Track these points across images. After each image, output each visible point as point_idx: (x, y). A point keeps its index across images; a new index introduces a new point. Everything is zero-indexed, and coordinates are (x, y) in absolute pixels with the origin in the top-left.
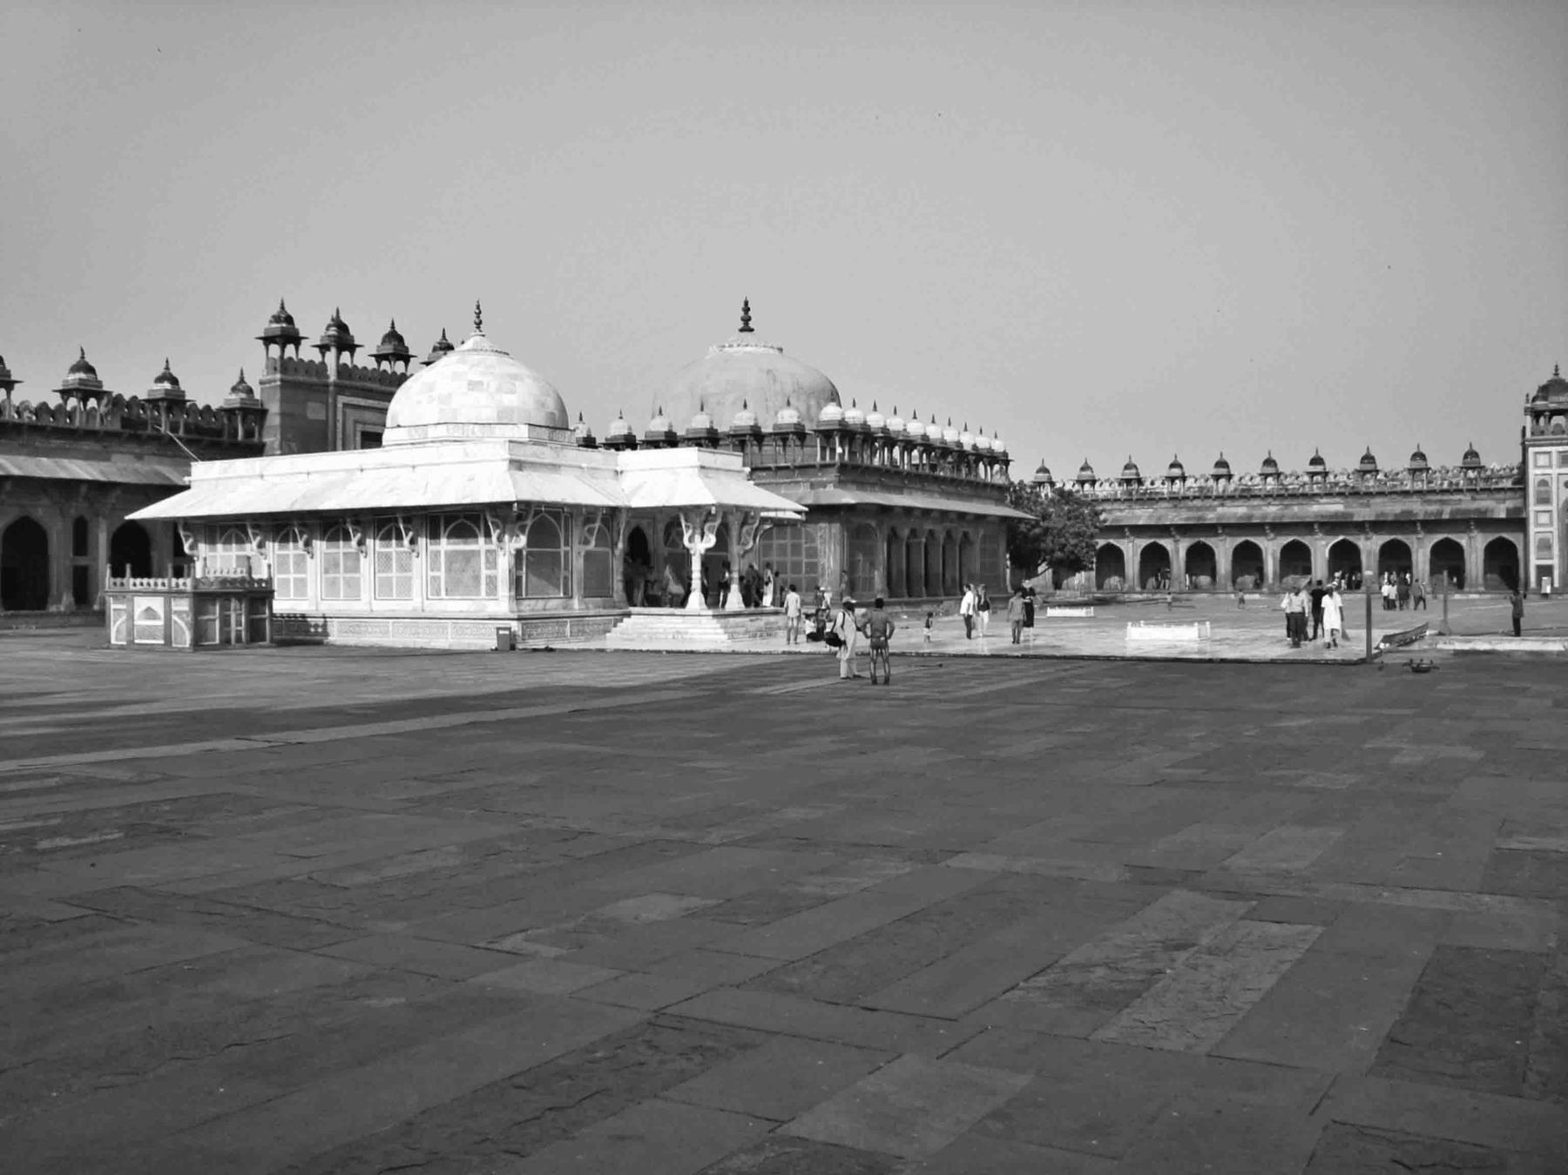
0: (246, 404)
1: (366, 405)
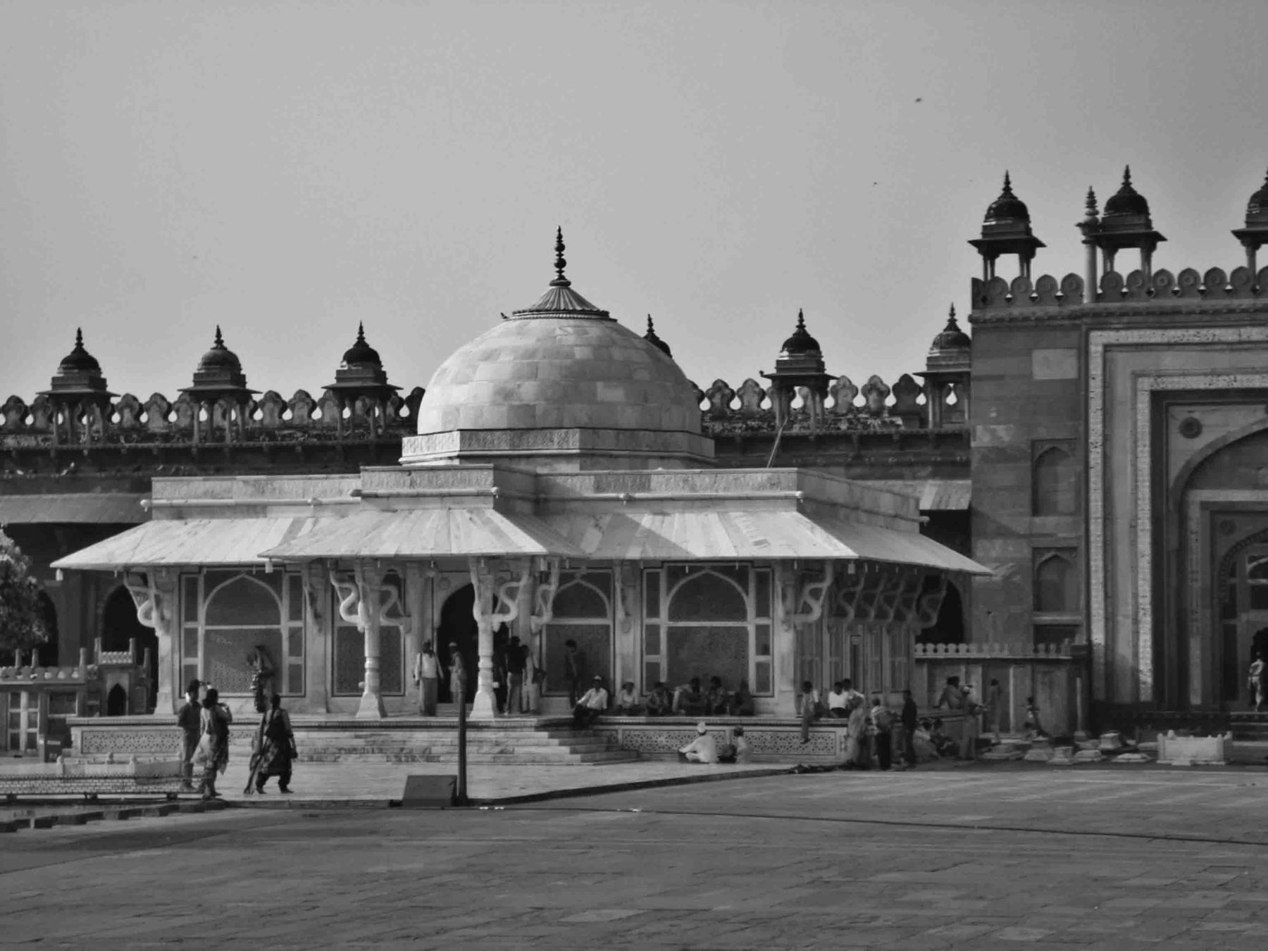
0: (941, 366)
1: (1165, 340)
